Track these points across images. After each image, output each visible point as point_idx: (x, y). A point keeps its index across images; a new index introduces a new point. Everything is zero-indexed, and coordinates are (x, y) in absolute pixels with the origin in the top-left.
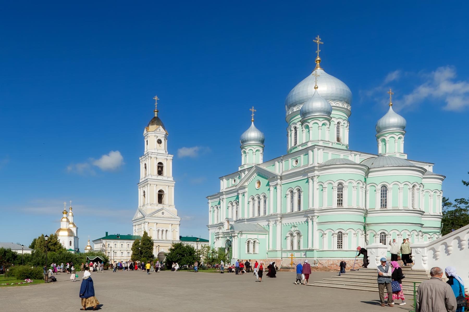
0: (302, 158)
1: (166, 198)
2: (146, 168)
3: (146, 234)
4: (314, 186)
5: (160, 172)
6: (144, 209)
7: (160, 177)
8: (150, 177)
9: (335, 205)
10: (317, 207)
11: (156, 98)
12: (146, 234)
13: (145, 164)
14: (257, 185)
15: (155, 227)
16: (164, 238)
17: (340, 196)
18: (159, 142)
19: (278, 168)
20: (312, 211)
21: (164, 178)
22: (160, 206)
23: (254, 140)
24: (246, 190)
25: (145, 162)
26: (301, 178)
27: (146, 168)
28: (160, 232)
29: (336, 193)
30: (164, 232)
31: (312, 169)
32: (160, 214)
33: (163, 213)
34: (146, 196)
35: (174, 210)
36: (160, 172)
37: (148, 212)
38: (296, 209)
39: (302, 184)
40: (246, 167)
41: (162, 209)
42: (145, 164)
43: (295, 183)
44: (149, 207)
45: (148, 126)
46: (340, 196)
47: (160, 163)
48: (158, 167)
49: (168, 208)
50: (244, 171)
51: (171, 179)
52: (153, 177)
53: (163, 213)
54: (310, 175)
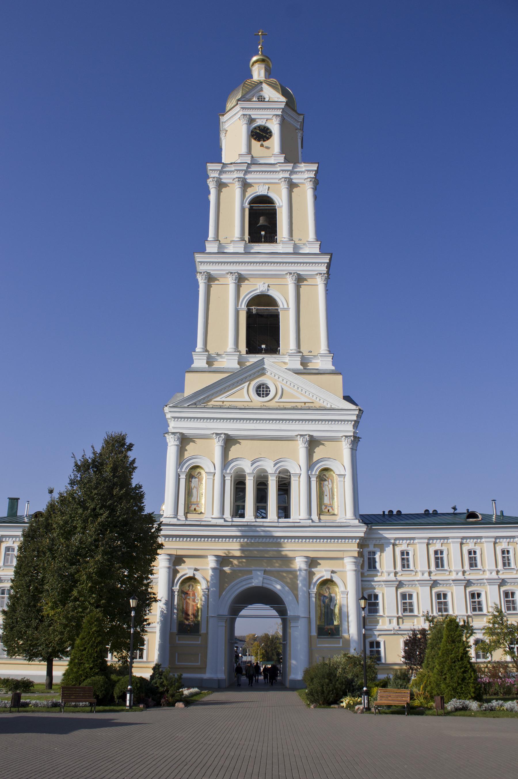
18: (261, 134)
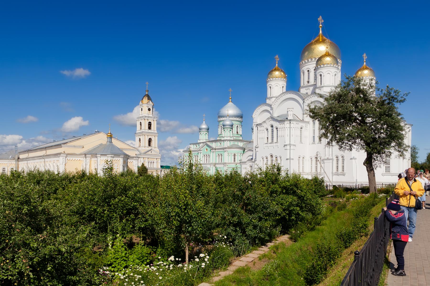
0: (222, 143)
1: (153, 143)
2: (141, 124)
3: (143, 164)
4: (225, 154)
5: (150, 128)
6: (140, 149)
7: (150, 131)
8: (144, 131)
9: (233, 162)
10: (227, 162)
11: (147, 83)
12: (143, 164)
13: (141, 123)
14: (206, 150)
15: (147, 160)
16: (152, 167)
17: (234, 158)
18: (149, 110)
19: (214, 145)
20: (226, 163)
21: (152, 131)
22: (150, 148)
23: (205, 129)
24: (202, 152)
25: (141, 121)
26: (222, 150)
27: (141, 124)
28: (150, 163)
29: (233, 157)
30: (152, 163)
31: (225, 148)
32: (150, 153)
33: (151, 152)
34: (141, 141)
35: (157, 150)
36: (150, 128)
37: (143, 152)
38: (220, 162)
39: (222, 153)
40: (201, 141)
41: (151, 150)
42: (141, 123)
43: (220, 152)
44: (144, 148)
45: (142, 99)
46: (234, 158)
47: (150, 122)
48: (149, 125)
49: (154, 149)
50: (201, 143)
51: (156, 132)
52: (146, 131)
53: (151, 152)
54: (225, 150)
